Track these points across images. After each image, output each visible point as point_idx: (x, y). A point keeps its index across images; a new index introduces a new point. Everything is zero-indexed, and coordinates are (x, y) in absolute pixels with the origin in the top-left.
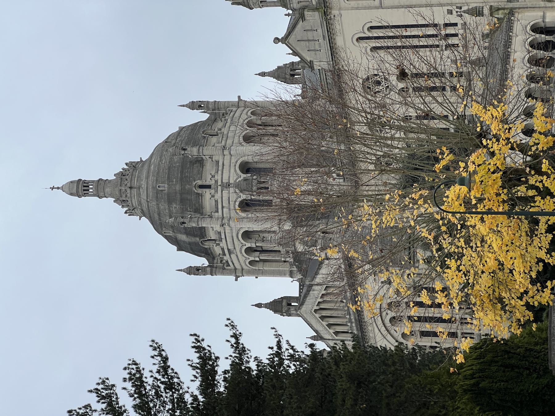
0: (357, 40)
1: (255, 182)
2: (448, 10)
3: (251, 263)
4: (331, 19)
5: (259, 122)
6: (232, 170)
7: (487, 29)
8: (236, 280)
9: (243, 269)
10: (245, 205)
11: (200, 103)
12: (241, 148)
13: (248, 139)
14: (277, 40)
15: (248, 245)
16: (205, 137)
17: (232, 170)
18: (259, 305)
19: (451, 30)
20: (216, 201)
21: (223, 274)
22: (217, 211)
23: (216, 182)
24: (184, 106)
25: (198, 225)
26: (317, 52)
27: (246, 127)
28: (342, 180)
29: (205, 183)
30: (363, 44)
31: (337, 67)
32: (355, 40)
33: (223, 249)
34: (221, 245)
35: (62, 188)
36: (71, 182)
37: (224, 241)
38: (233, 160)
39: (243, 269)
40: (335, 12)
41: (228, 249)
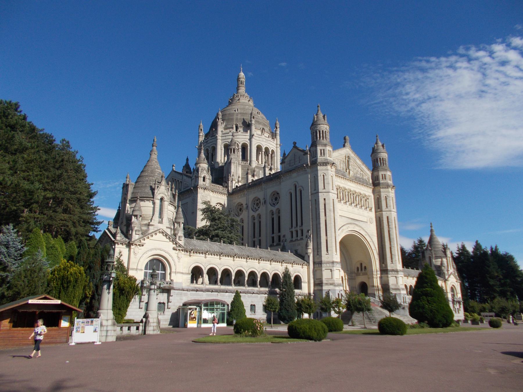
0: (295, 184)
1: (234, 147)
6: (243, 140)
7: (299, 252)
13: (259, 148)
14: (295, 143)
15: (209, 150)
17: (243, 140)
18: (187, 160)
20: (228, 133)
23: (238, 133)
28: (233, 188)
30: (293, 188)
32: (295, 183)
37: (211, 138)
40: (309, 170)
41: (207, 141)
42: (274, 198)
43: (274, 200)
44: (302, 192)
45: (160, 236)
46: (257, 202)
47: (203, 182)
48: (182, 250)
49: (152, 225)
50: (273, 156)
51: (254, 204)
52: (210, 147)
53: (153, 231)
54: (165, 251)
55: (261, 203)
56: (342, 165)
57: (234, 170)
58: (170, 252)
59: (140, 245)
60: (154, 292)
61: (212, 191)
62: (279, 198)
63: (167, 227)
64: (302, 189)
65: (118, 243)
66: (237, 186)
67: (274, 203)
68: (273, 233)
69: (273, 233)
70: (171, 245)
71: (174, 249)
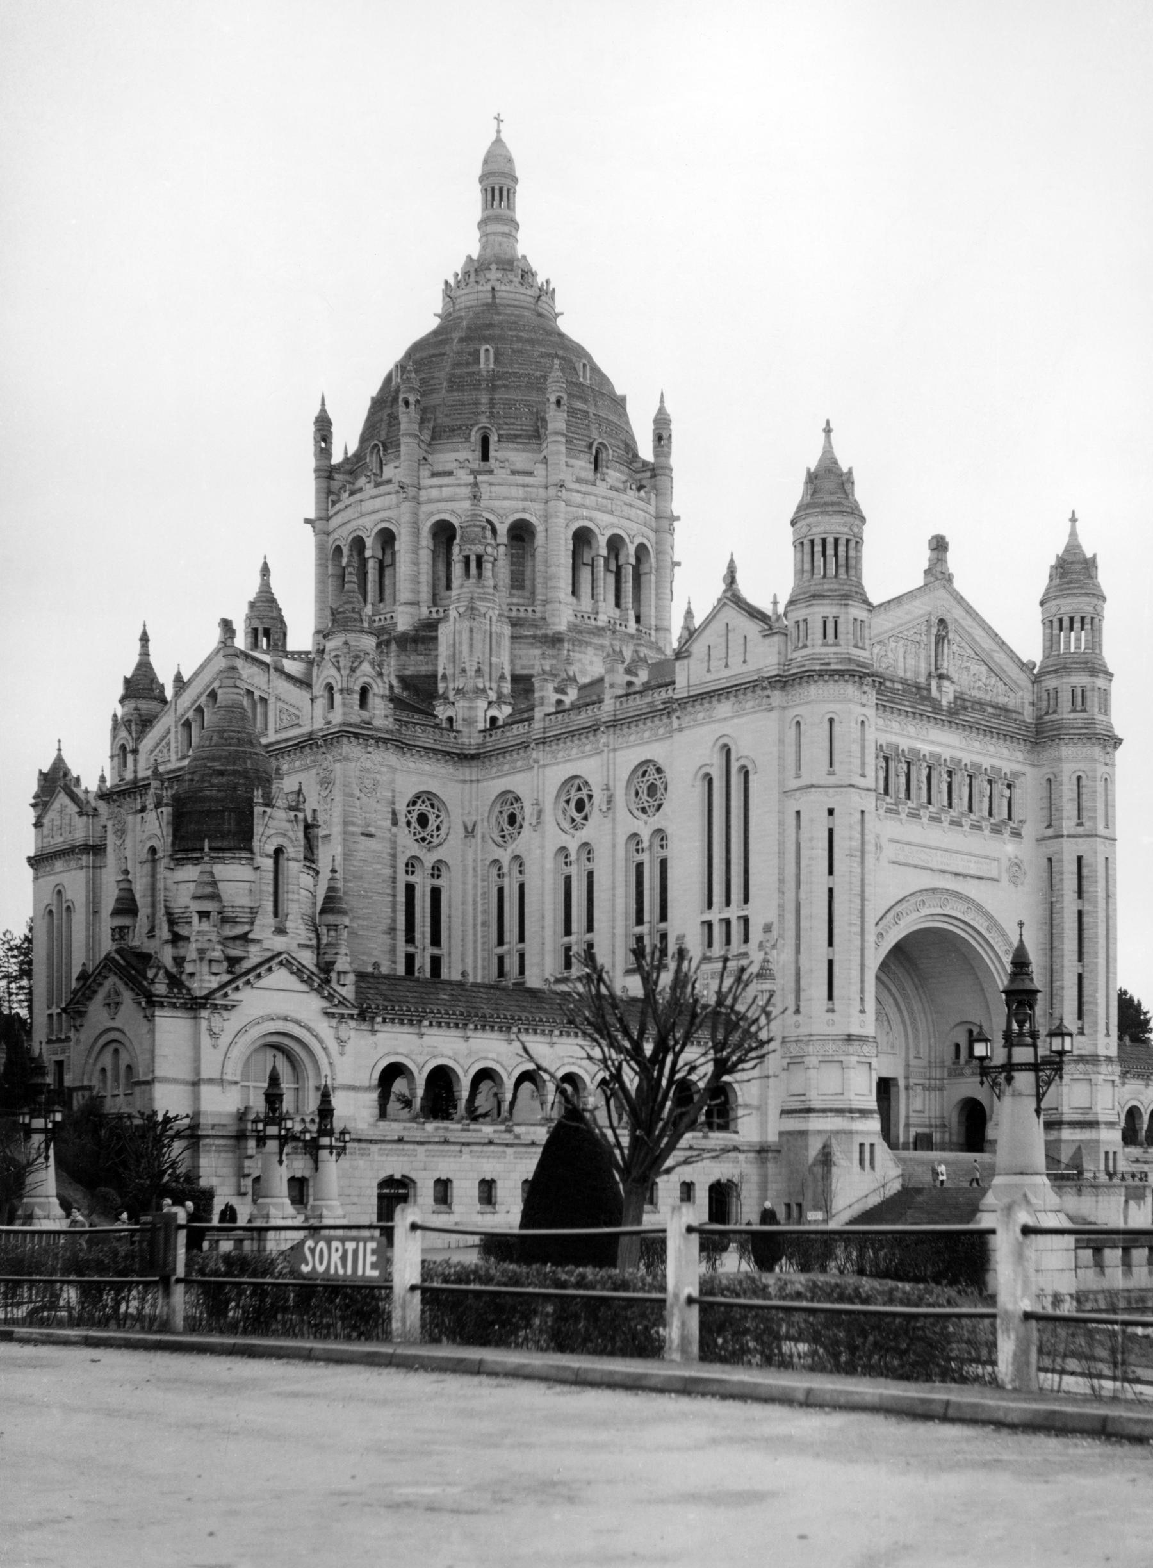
0: (725, 745)
1: (479, 549)
2: (772, 924)
3: (338, 549)
4: (764, 689)
5: (622, 561)
8: (307, 521)
9: (328, 534)
10: (444, 533)
11: (665, 436)
12: (561, 522)
13: (582, 538)
15: (369, 542)
16: (590, 446)
19: (736, 929)
21: (318, 491)
22: (434, 475)
24: (662, 401)
25: (403, 435)
26: (706, 664)
27: (609, 533)
28: (481, 726)
29: (492, 447)
31: (675, 706)
33: (360, 490)
34: (368, 486)
35: (498, 142)
36: (510, 160)
38: (538, 507)
39: (328, 534)
41: (361, 501)
42: (645, 787)
43: (645, 797)
44: (751, 777)
45: (280, 977)
46: (580, 795)
47: (363, 712)
48: (351, 1017)
49: (258, 941)
50: (644, 568)
51: (568, 802)
52: (373, 534)
53: (259, 960)
54: (298, 1022)
55: (596, 800)
56: (911, 662)
57: (484, 653)
58: (311, 1024)
59: (226, 1008)
60: (331, 1153)
61: (397, 746)
62: (666, 789)
63: (300, 945)
64: (750, 768)
65: (162, 1003)
66: (494, 720)
67: (646, 805)
68: (640, 921)
69: (640, 921)
70: (315, 1003)
71: (329, 1015)
